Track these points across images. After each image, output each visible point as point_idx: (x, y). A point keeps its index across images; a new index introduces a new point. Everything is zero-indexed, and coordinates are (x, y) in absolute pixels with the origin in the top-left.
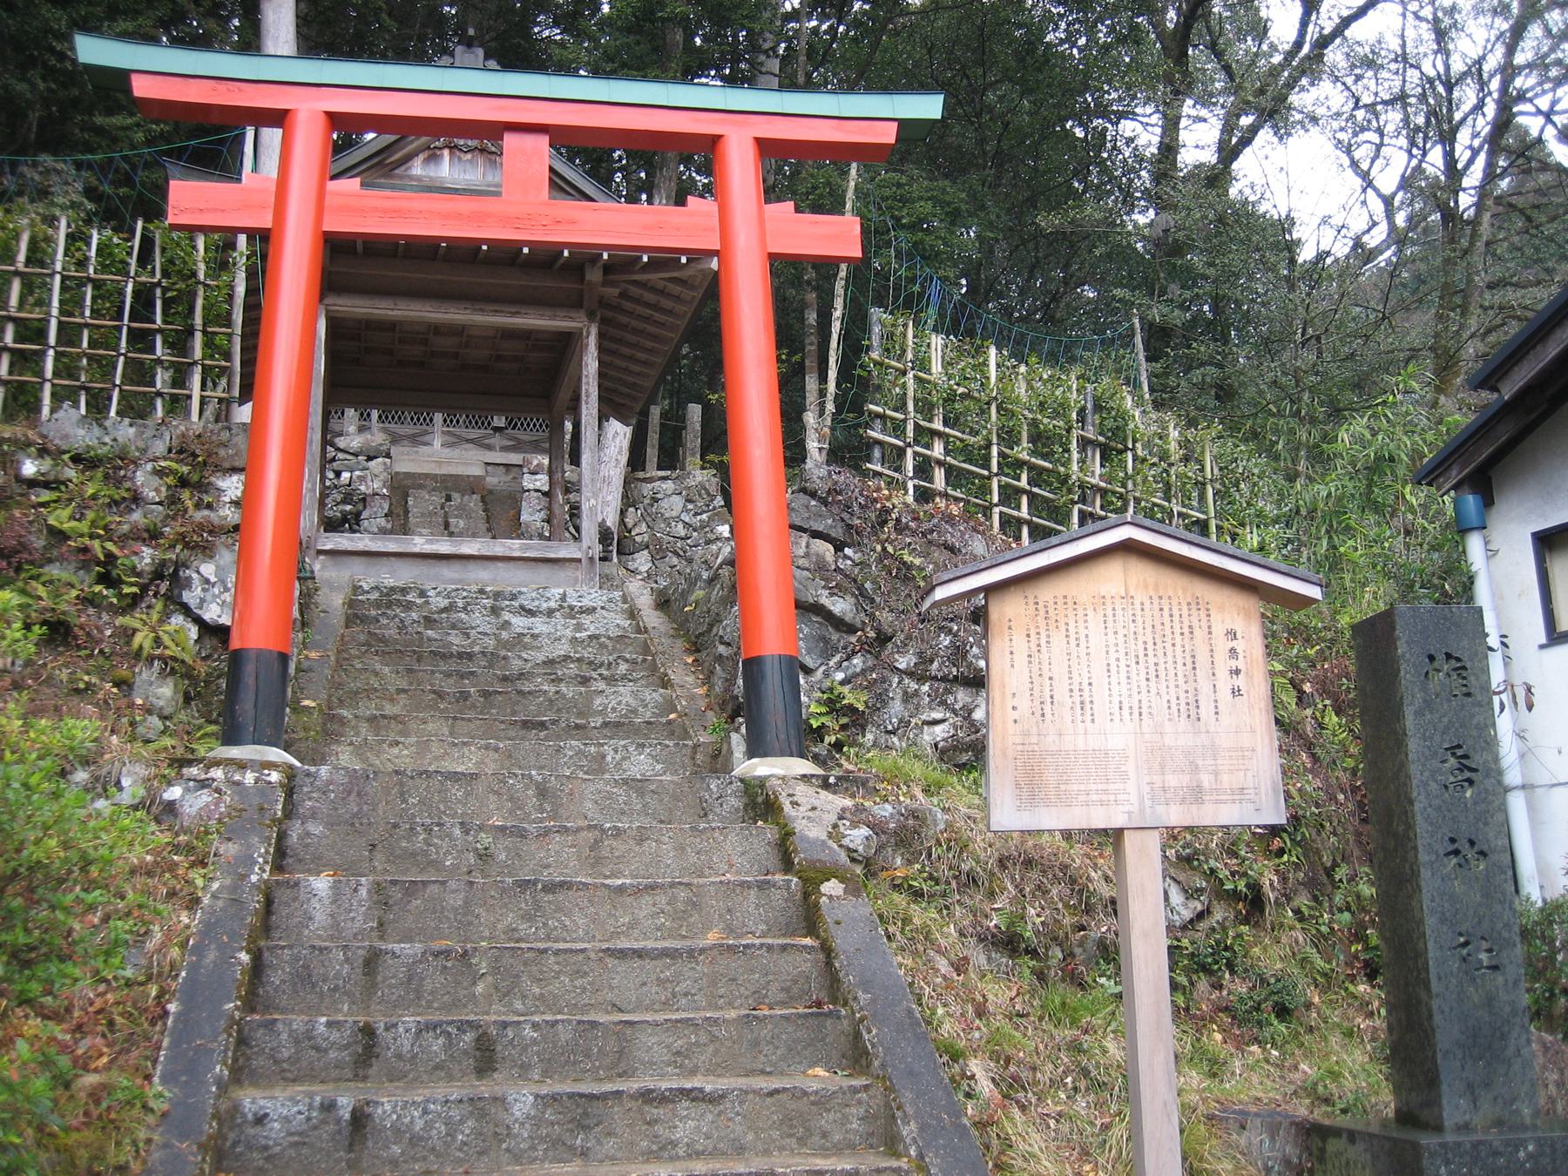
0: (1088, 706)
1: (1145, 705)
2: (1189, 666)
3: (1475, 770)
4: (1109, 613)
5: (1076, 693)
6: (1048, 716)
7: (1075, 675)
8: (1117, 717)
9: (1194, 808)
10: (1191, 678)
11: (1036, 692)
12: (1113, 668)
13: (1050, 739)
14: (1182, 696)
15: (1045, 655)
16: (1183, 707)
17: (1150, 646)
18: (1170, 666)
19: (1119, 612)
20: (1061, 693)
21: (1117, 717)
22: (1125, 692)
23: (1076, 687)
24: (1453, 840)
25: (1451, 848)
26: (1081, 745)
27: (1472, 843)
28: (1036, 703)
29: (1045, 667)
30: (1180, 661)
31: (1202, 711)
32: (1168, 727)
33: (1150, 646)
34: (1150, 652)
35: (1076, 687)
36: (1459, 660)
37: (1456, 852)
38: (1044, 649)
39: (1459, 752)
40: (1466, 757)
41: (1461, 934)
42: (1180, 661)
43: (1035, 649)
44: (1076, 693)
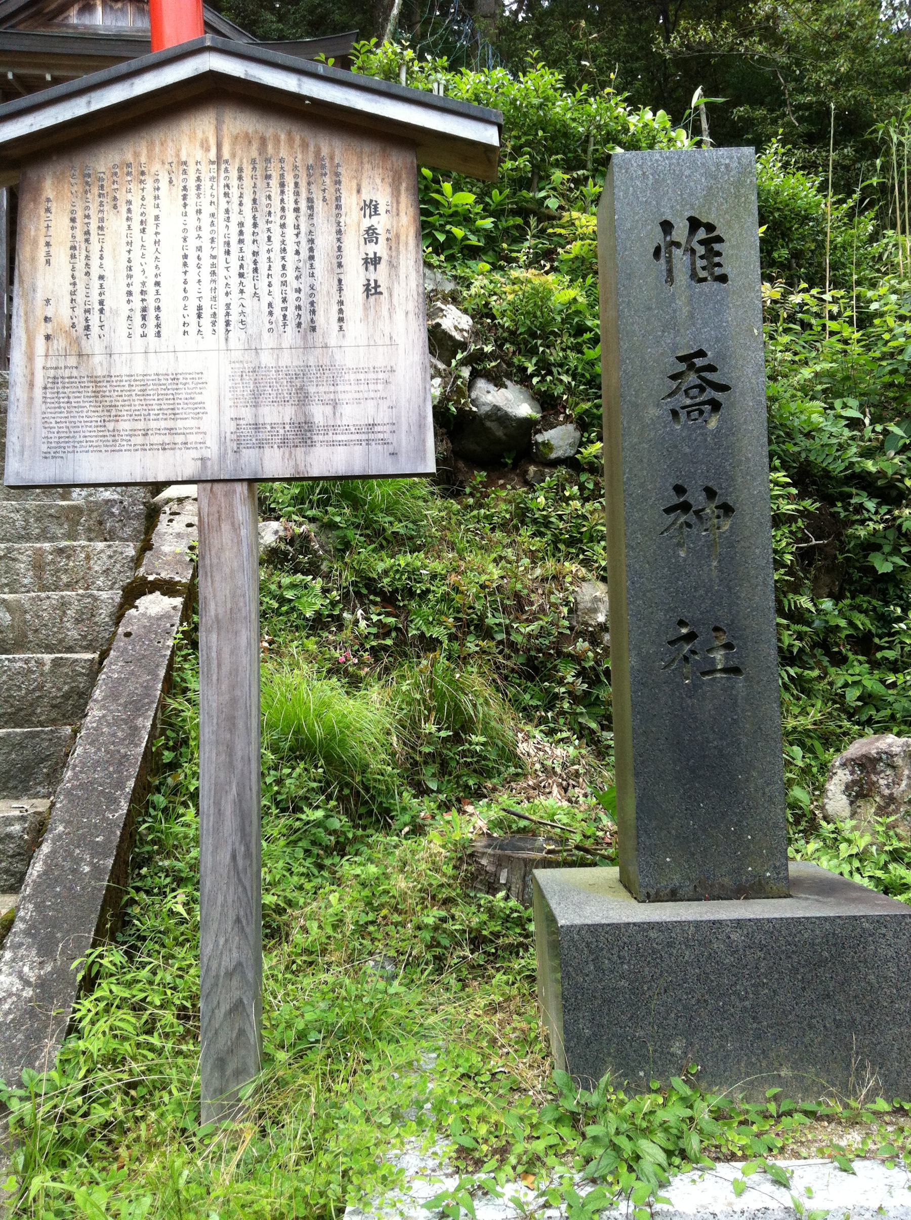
0: (152, 314)
1: (235, 311)
2: (304, 253)
3: (724, 388)
4: (192, 184)
5: (137, 297)
6: (95, 330)
7: (137, 271)
8: (193, 329)
9: (299, 451)
10: (305, 271)
11: (80, 297)
12: (192, 261)
13: (96, 360)
14: (292, 296)
15: (95, 246)
16: (291, 313)
17: (248, 229)
18: (276, 256)
19: (206, 184)
20: (115, 299)
21: (193, 329)
22: (207, 295)
23: (136, 289)
24: (680, 490)
25: (676, 500)
26: (139, 369)
27: (711, 493)
28: (80, 311)
29: (95, 262)
30: (291, 248)
31: (320, 319)
32: (268, 341)
33: (248, 229)
34: (248, 237)
35: (136, 289)
36: (710, 228)
37: (685, 507)
38: (94, 238)
39: (699, 362)
40: (711, 368)
41: (682, 623)
42: (291, 248)
43: (80, 237)
44: (137, 297)
